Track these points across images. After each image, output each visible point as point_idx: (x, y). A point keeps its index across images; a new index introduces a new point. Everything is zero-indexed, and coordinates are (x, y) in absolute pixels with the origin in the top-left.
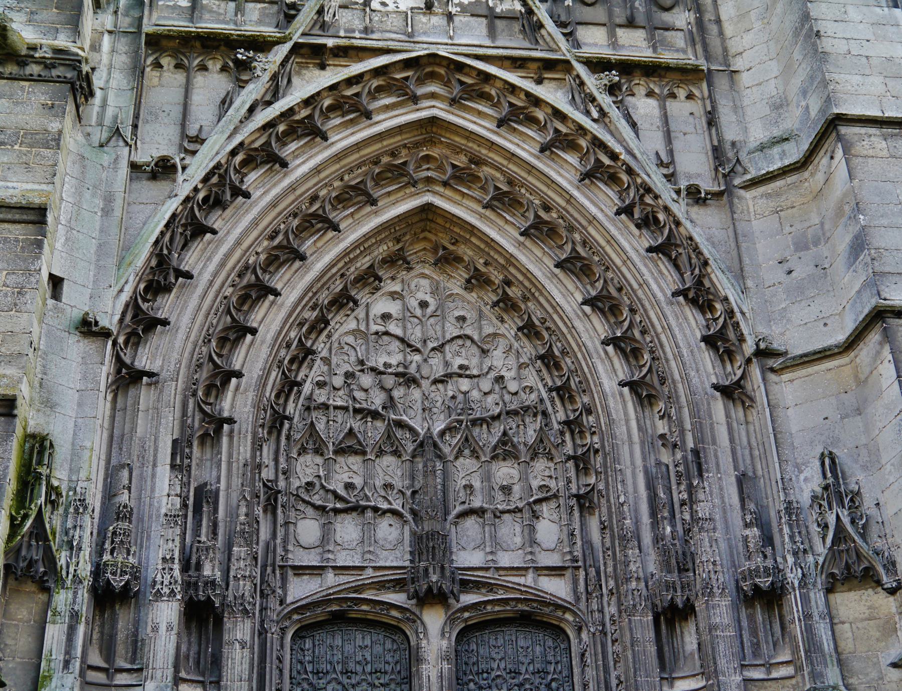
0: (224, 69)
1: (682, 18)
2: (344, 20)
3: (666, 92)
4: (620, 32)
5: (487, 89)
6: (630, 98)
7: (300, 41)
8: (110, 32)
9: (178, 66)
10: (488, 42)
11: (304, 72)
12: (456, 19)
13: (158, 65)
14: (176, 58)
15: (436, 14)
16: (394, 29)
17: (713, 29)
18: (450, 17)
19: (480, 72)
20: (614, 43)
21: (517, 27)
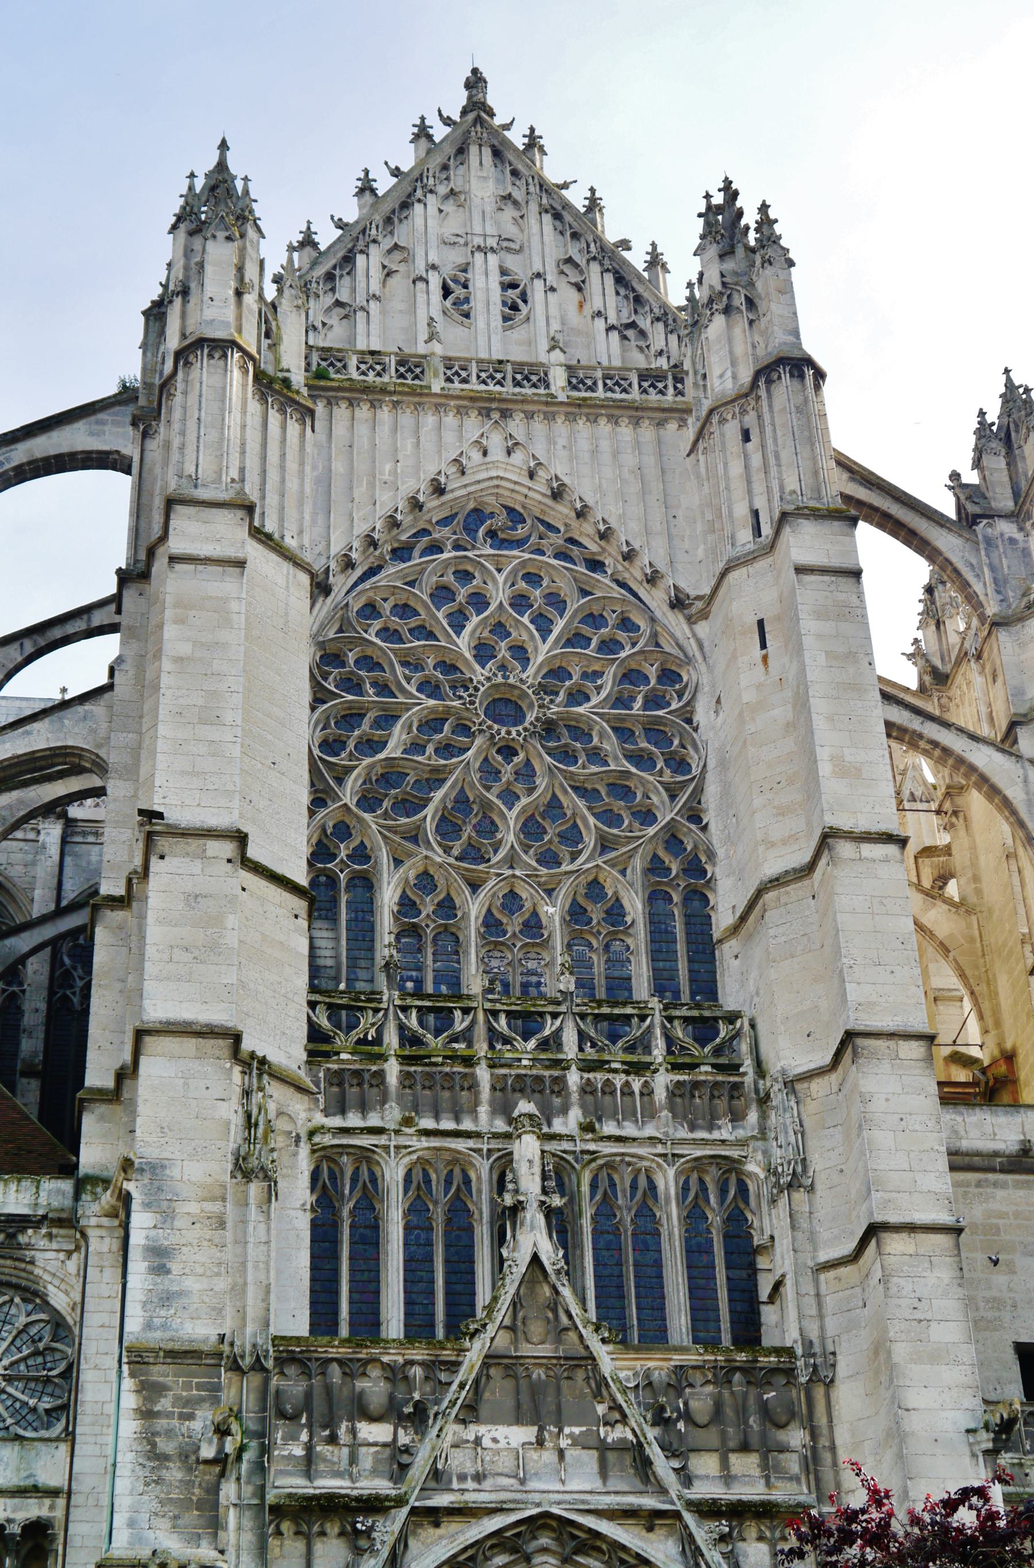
0: (342, 1534)
1: (796, 1437)
2: (456, 1463)
3: (777, 1534)
4: (733, 1458)
5: (598, 1543)
6: (740, 1544)
7: (417, 1504)
8: (235, 1505)
9: (297, 1533)
10: (597, 1484)
11: (420, 1531)
12: (568, 1454)
13: (279, 1533)
14: (298, 1524)
15: (547, 1449)
16: (506, 1471)
17: (827, 1457)
18: (561, 1453)
19: (590, 1531)
20: (727, 1478)
21: (628, 1459)
